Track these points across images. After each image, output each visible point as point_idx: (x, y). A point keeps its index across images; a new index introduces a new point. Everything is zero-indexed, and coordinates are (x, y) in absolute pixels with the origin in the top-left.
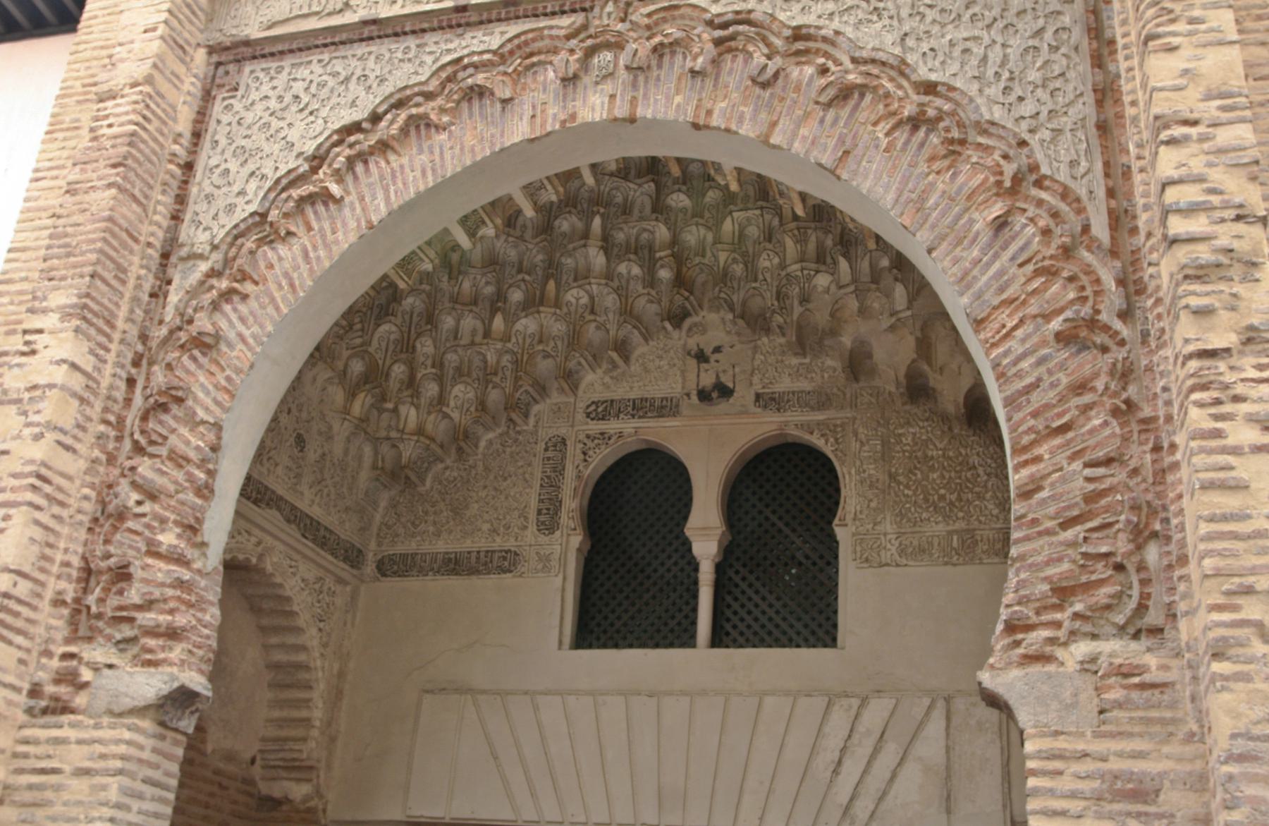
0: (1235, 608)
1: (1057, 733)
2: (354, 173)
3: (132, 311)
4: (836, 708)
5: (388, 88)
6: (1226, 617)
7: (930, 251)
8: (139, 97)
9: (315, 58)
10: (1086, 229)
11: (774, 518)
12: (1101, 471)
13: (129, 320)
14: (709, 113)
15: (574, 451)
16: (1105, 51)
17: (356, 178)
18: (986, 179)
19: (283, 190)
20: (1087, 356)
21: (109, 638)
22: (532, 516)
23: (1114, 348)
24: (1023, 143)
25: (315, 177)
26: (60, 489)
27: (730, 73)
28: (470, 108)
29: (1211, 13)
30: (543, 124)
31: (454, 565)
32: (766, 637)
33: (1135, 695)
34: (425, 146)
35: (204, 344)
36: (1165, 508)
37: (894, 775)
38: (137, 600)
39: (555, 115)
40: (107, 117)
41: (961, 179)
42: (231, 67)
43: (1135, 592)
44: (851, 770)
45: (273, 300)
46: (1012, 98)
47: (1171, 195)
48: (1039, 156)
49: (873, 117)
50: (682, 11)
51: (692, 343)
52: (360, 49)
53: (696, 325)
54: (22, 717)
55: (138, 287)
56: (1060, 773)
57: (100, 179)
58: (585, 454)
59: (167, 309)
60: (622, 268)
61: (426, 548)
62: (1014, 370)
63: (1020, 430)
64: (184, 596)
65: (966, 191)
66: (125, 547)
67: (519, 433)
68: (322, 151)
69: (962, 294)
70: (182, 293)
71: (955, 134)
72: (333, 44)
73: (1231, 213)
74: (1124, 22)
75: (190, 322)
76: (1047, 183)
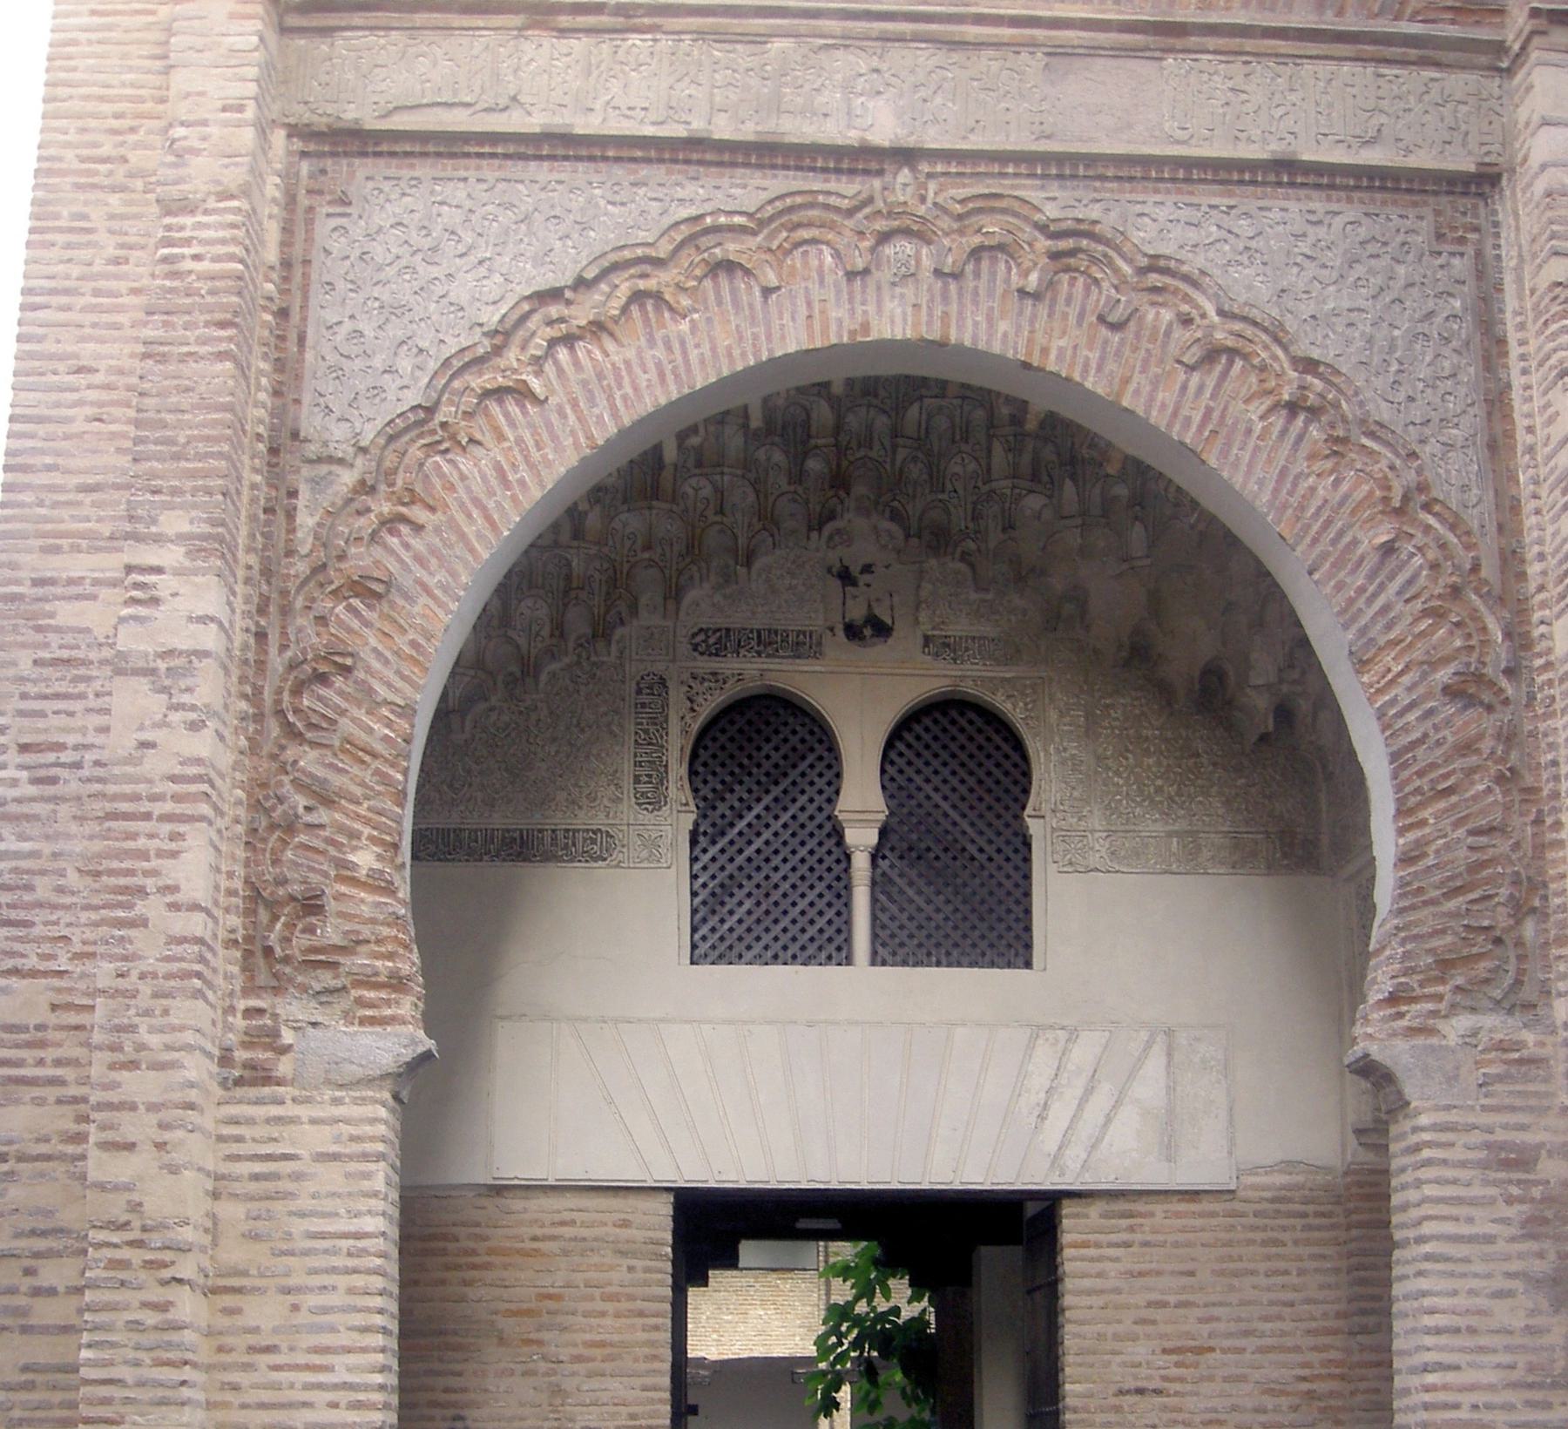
1: (1448, 1108)
2: (556, 362)
3: (252, 536)
7: (1310, 573)
9: (472, 175)
10: (1475, 568)
12: (1483, 840)
14: (1045, 351)
18: (1371, 493)
19: (453, 377)
20: (1471, 713)
21: (304, 989)
23: (1499, 707)
24: (1413, 455)
25: (502, 363)
26: (220, 795)
27: (1068, 301)
33: (1513, 1070)
34: (659, 335)
35: (366, 590)
36: (1545, 885)
38: (337, 939)
39: (840, 321)
41: (1344, 487)
42: (329, 163)
43: (1512, 966)
45: (463, 536)
46: (1401, 397)
48: (1429, 475)
50: (1003, 204)
52: (541, 172)
54: (219, 1093)
56: (1452, 1145)
57: (203, 341)
59: (300, 534)
62: (1400, 723)
65: (1350, 505)
66: (298, 870)
68: (508, 324)
69: (1346, 627)
71: (1340, 433)
75: (342, 557)
76: (1437, 508)
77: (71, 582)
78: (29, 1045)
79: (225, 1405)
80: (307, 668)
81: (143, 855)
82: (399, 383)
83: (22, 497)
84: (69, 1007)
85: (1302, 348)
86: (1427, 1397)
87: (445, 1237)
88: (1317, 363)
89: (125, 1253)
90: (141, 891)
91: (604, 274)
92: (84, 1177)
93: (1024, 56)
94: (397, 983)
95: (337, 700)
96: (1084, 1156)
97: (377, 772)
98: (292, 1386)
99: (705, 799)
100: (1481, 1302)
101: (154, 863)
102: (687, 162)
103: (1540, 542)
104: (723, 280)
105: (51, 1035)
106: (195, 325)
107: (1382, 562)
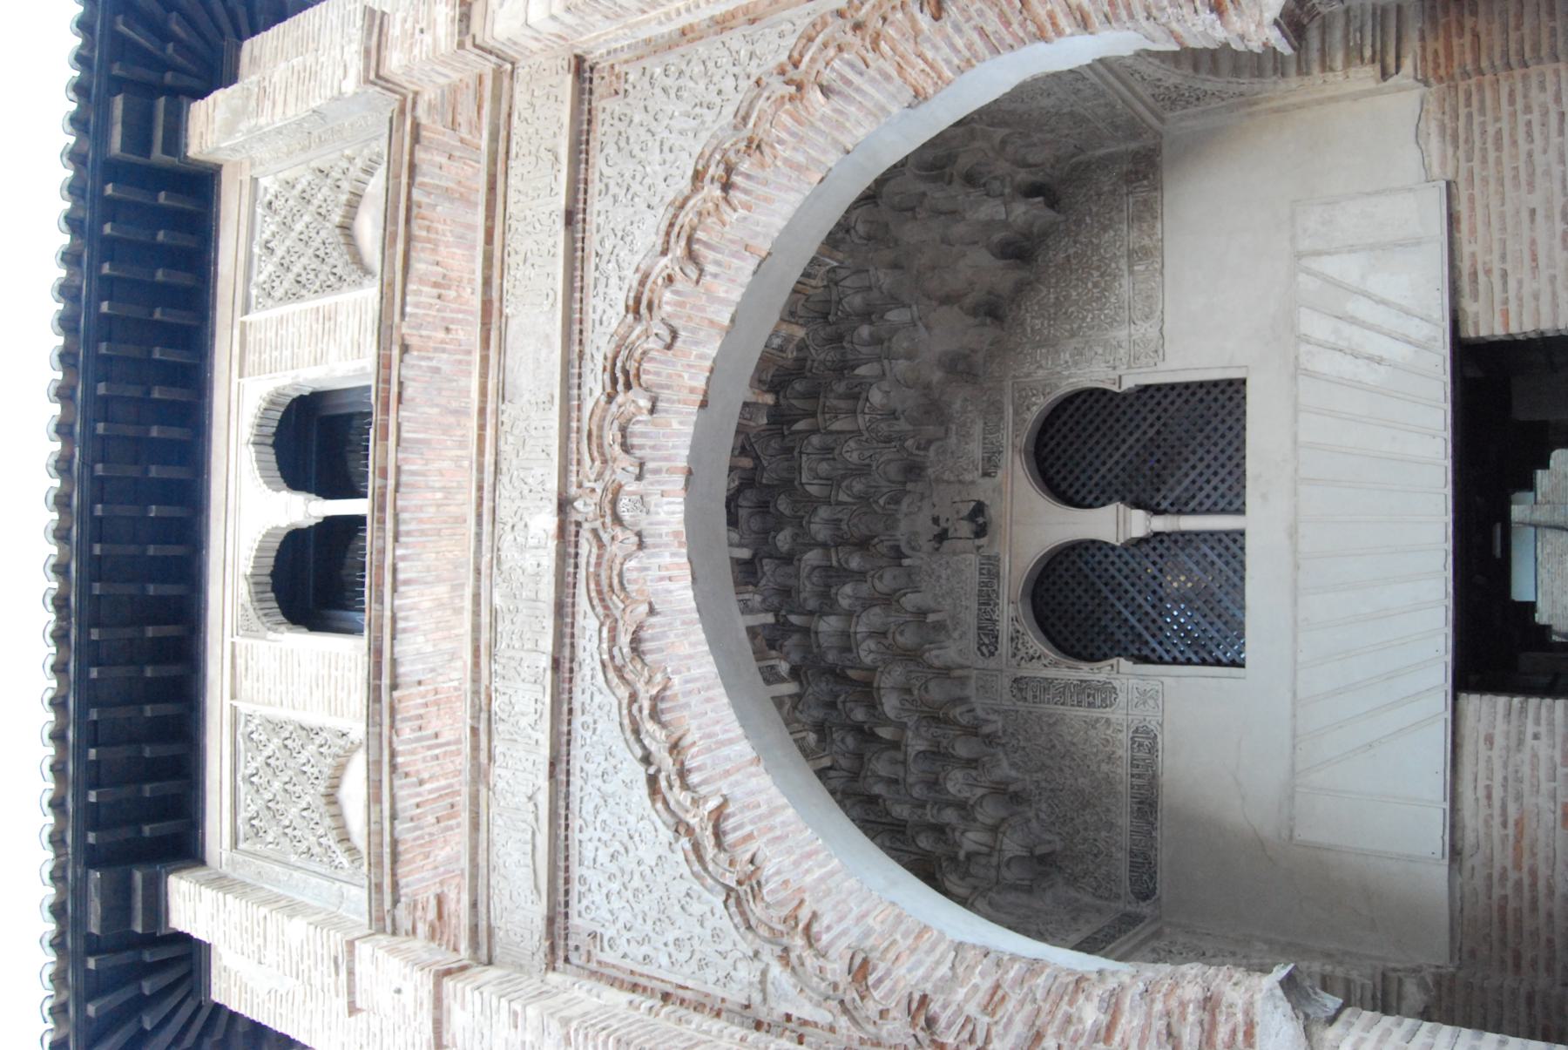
4: (1310, 367)
5: (619, 747)
7: (848, 152)
8: (581, 1032)
9: (575, 835)
11: (1110, 463)
14: (692, 390)
16: (690, 36)
19: (706, 869)
22: (1095, 713)
24: (758, 83)
25: (698, 830)
27: (658, 374)
28: (651, 652)
30: (679, 566)
32: (1234, 462)
34: (682, 700)
35: (861, 971)
37: (1383, 302)
41: (784, 135)
42: (572, 943)
45: (822, 879)
46: (718, 101)
49: (718, 228)
51: (926, 544)
52: (576, 780)
53: (909, 543)
58: (1032, 658)
60: (845, 603)
61: (1125, 840)
62: (968, 54)
63: (1021, 34)
64: (1164, 990)
67: (1004, 731)
68: (671, 821)
74: (668, 17)
75: (835, 986)
80: (921, 1035)
82: (709, 915)
85: (685, 185)
87: (1502, 909)
91: (639, 740)
93: (504, 418)
94: (1210, 1003)
95: (949, 1012)
96: (1417, 321)
97: (1012, 987)
99: (1111, 649)
102: (571, 670)
104: (645, 646)
107: (839, 93)
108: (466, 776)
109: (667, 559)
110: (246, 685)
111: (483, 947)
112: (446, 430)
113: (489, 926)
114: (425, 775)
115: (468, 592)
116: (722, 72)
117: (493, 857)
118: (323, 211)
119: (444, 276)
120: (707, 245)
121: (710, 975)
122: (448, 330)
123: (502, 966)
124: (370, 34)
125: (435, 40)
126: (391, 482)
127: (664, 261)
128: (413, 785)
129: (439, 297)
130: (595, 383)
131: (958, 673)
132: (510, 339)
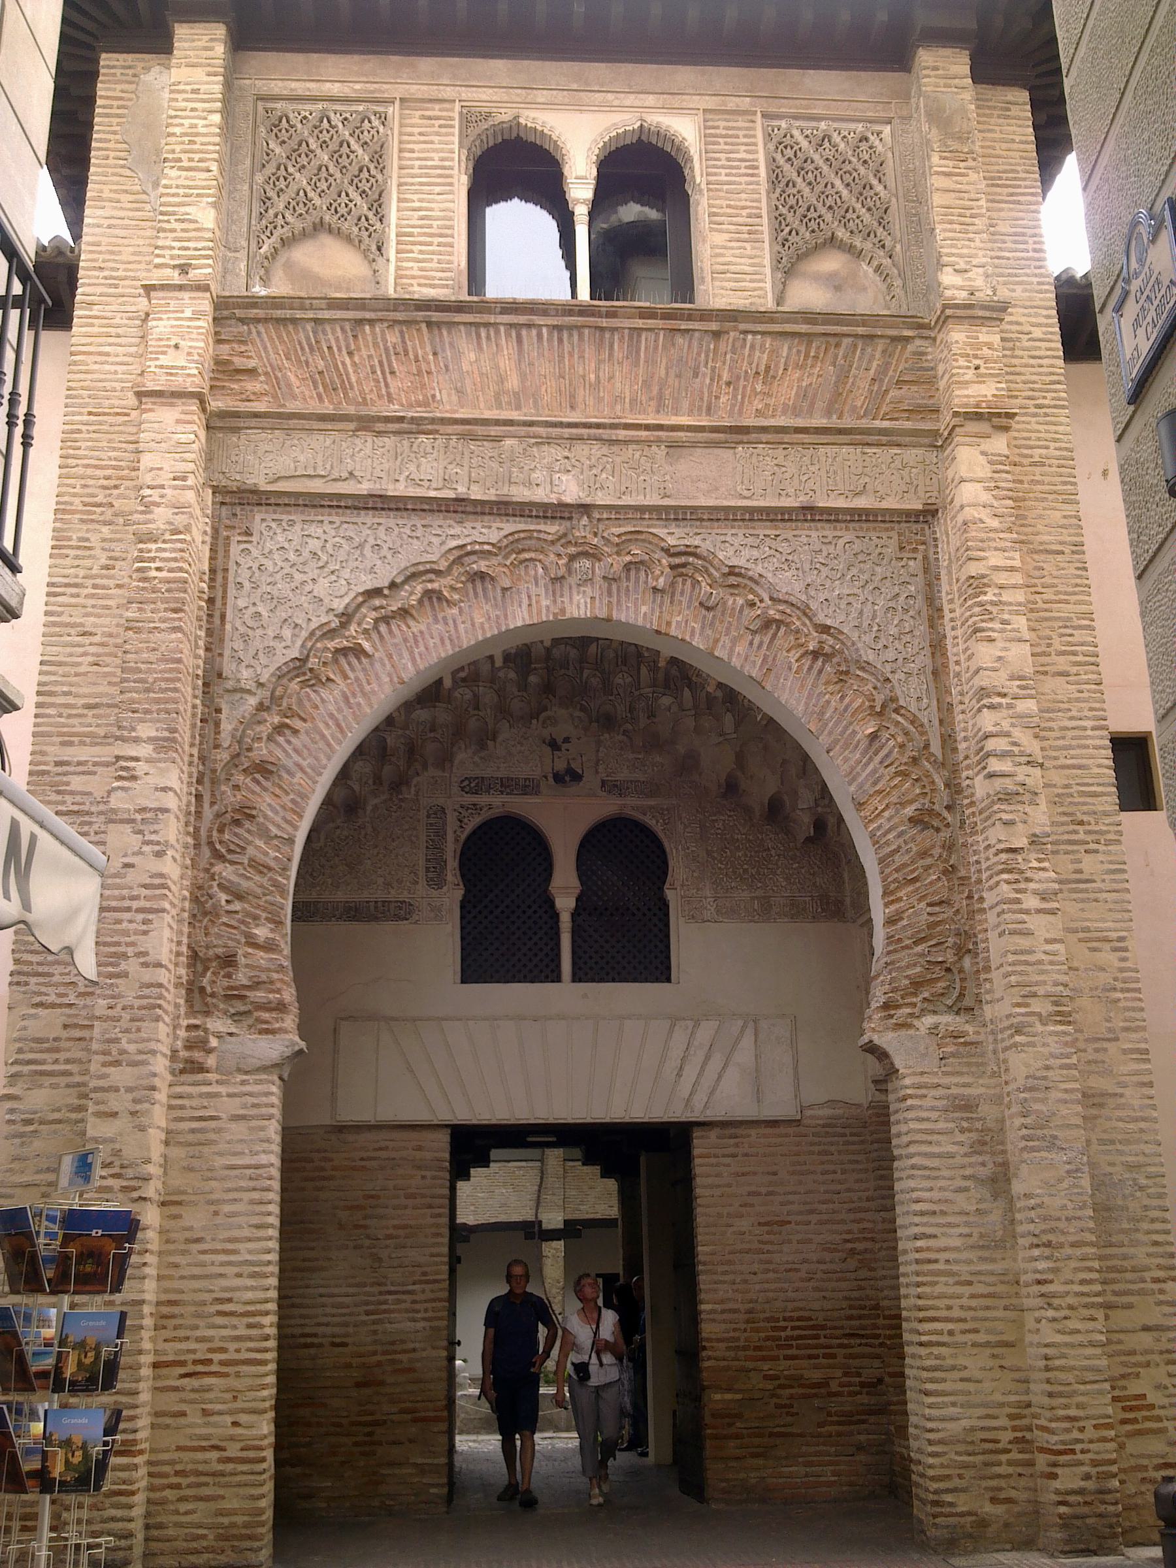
0: (1027, 1005)
1: (922, 1073)
6: (1022, 1010)
9: (326, 519)
10: (927, 746)
12: (937, 909)
13: (192, 745)
14: (669, 624)
15: (451, 818)
17: (381, 637)
22: (422, 873)
27: (682, 593)
29: (1014, 618)
30: (539, 613)
31: (354, 913)
33: (961, 1049)
35: (264, 769)
38: (245, 982)
39: (548, 607)
40: (153, 559)
41: (847, 700)
42: (238, 509)
43: (958, 986)
44: (690, 1074)
45: (323, 736)
46: (880, 646)
47: (991, 745)
48: (899, 693)
51: (546, 733)
52: (369, 518)
53: (549, 718)
54: (169, 1077)
55: (194, 715)
65: (850, 710)
68: (350, 611)
69: (850, 784)
70: (235, 722)
72: (339, 507)
73: (1023, 759)
74: (951, 601)
75: (249, 750)
77: (79, 763)
78: (48, 1050)
79: (170, 1277)
81: (126, 933)
83: (48, 711)
84: (76, 1026)
85: (821, 618)
86: (917, 1256)
88: (830, 627)
89: (110, 1182)
90: (124, 956)
91: (408, 579)
92: (84, 1133)
94: (281, 1007)
97: (270, 879)
98: (213, 1264)
100: (948, 1195)
101: (132, 938)
103: (965, 730)
105: (63, 1044)
106: (158, 611)
108: (364, 411)
109: (545, 602)
110: (415, 117)
111: (221, 425)
112: (646, 384)
113: (240, 428)
114: (356, 359)
115: (515, 415)
116: (901, 648)
117: (297, 435)
118: (848, 216)
119: (774, 377)
120: (775, 636)
121: (238, 645)
122: (728, 384)
123: (209, 439)
124: (984, 308)
125: (967, 382)
126: (604, 322)
127: (767, 599)
128: (347, 347)
129: (757, 373)
130: (674, 536)
131: (447, 765)
132: (717, 451)
